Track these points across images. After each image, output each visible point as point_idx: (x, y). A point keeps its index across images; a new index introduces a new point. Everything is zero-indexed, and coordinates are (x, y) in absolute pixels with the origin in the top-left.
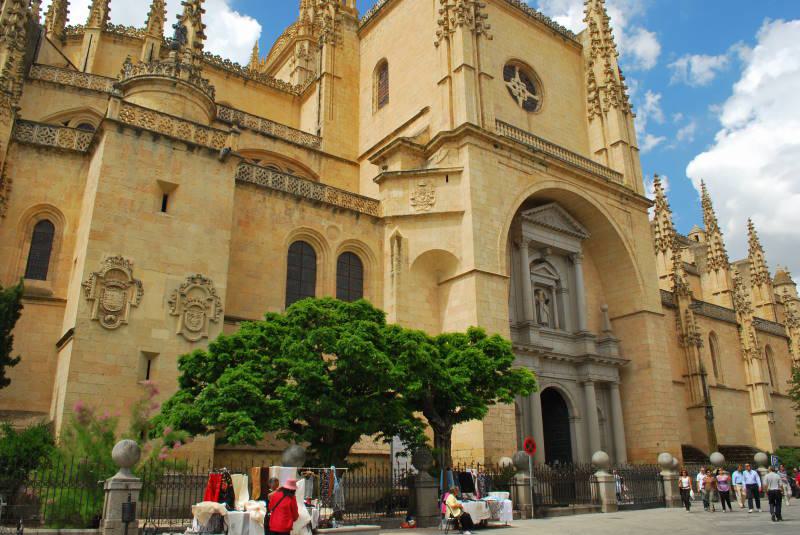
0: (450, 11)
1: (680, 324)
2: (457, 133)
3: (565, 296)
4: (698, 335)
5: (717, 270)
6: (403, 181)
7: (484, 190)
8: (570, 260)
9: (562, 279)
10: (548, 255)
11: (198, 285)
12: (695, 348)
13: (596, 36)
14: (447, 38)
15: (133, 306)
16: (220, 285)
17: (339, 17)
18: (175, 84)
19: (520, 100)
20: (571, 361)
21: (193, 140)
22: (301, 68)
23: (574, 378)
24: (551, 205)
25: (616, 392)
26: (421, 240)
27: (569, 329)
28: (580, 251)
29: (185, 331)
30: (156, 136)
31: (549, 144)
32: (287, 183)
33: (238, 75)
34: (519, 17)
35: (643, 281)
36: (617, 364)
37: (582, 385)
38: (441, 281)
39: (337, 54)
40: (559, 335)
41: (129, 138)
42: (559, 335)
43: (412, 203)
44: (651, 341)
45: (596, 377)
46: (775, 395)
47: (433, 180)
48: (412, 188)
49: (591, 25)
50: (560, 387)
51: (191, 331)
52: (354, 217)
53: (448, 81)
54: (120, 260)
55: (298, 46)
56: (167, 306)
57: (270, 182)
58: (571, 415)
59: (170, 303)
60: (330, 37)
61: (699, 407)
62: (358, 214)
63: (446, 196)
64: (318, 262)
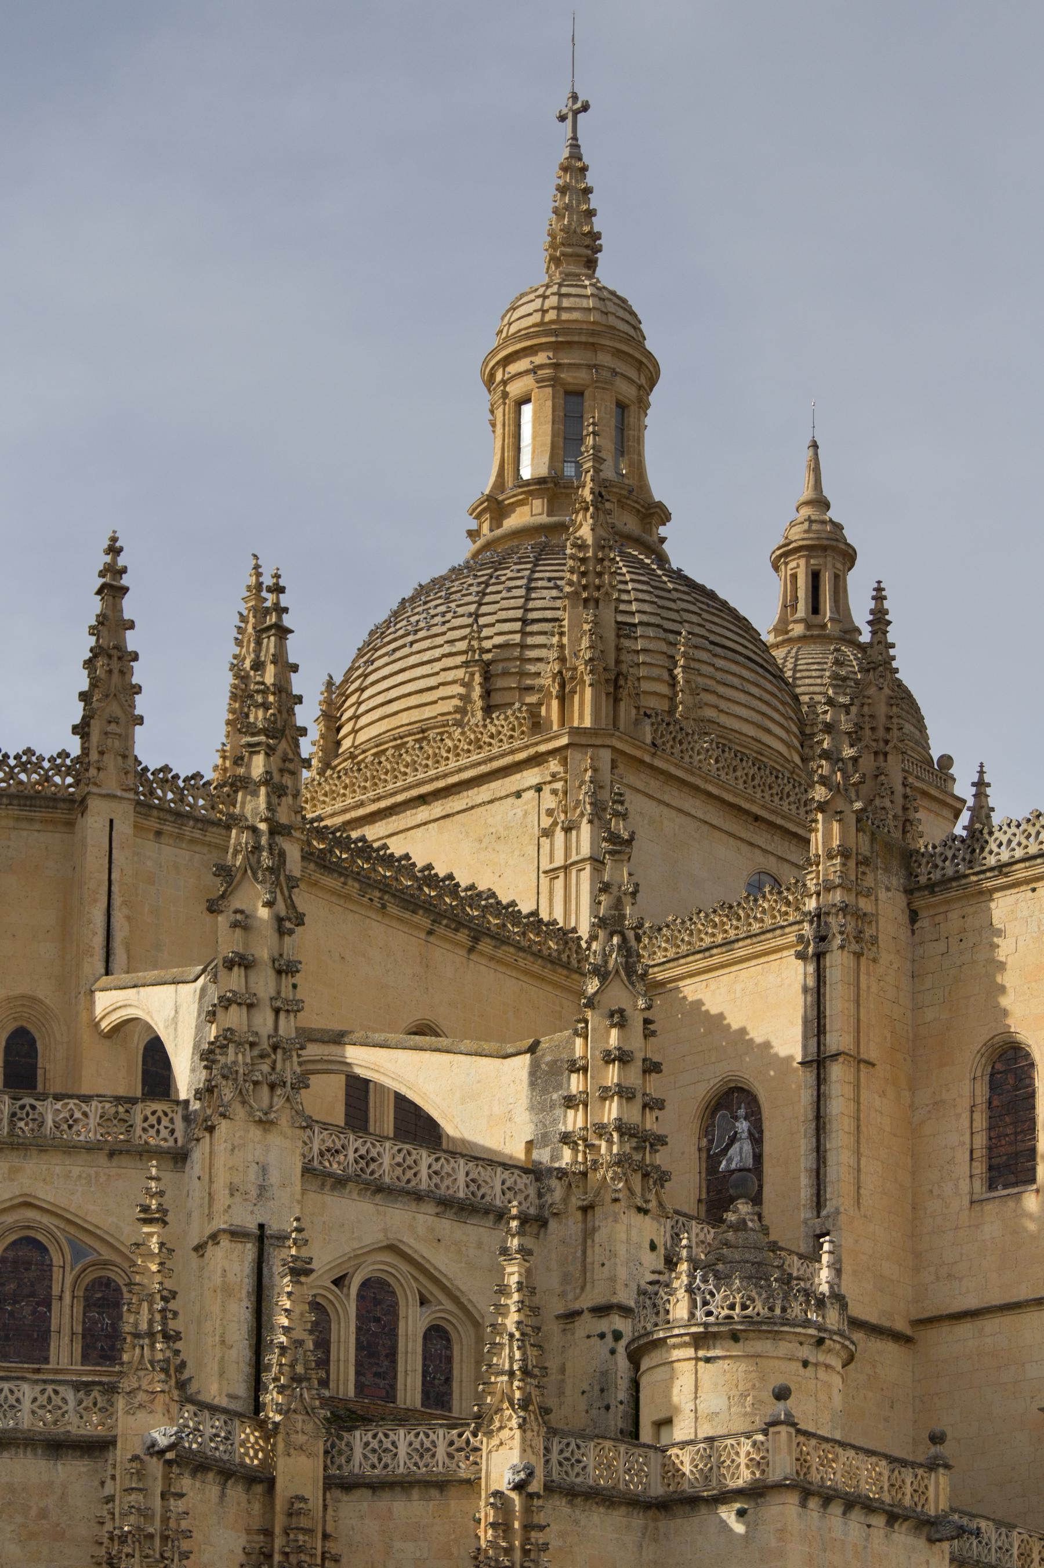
18: (820, 1342)
33: (458, 923)
39: (863, 978)
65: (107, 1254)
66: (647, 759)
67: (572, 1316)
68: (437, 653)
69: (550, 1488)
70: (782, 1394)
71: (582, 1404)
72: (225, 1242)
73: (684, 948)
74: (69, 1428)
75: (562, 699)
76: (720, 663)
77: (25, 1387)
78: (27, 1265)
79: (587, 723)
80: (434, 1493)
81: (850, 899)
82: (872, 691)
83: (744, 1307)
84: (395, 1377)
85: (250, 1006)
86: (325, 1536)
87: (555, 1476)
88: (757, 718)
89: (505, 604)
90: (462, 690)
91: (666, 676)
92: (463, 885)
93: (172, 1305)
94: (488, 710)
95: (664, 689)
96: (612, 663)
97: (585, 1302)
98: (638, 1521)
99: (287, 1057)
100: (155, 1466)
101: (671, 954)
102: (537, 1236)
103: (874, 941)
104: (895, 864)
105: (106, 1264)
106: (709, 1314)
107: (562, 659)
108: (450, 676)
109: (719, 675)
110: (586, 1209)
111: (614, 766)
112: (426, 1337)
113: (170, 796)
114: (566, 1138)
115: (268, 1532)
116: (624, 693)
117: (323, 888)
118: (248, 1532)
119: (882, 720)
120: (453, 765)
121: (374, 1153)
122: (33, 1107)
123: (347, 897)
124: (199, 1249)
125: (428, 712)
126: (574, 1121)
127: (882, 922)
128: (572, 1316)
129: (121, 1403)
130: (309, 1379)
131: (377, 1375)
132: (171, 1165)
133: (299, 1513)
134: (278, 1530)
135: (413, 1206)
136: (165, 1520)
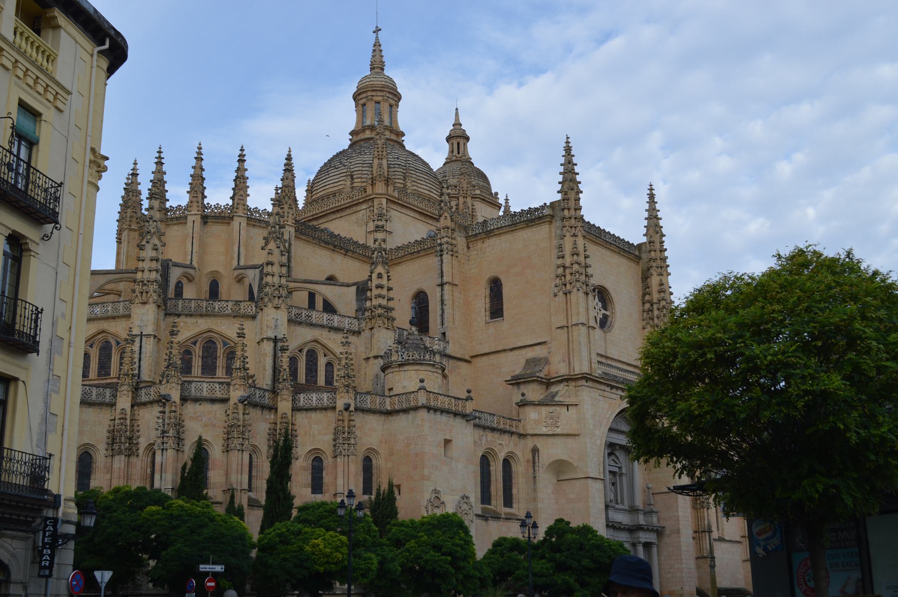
0: (568, 271)
2: (576, 377)
3: (624, 478)
6: (538, 408)
7: (592, 419)
8: (628, 450)
9: (623, 466)
10: (616, 450)
11: (465, 501)
12: (705, 509)
14: (566, 294)
16: (472, 500)
21: (454, 409)
23: (629, 540)
24: (620, 415)
26: (551, 451)
30: (443, 411)
31: (625, 371)
37: (634, 545)
38: (562, 478)
41: (432, 415)
43: (544, 424)
44: (680, 514)
45: (643, 540)
47: (558, 408)
48: (544, 410)
49: (650, 243)
52: (510, 435)
54: (436, 491)
55: (376, 202)
60: (450, 247)
61: (706, 557)
62: (512, 433)
63: (567, 420)
64: (492, 468)
66: (397, 201)
67: (367, 359)
68: (339, 172)
69: (356, 409)
70: (422, 381)
71: (371, 383)
72: (265, 341)
73: (406, 253)
74: (218, 396)
75: (372, 185)
76: (418, 174)
77: (205, 384)
78: (210, 348)
79: (380, 192)
80: (324, 411)
81: (450, 240)
82: (462, 180)
83: (413, 356)
84: (317, 377)
85: (273, 275)
86: (292, 424)
87: (358, 406)
88: (429, 189)
89: (357, 159)
90: (346, 183)
91: (402, 178)
92: (343, 237)
93: (246, 360)
94: (352, 188)
95: (401, 181)
96: (386, 176)
97: (372, 355)
98: (383, 418)
100: (240, 406)
101: (403, 254)
102: (358, 336)
103: (457, 252)
104: (462, 231)
106: (403, 358)
107: (372, 174)
108: (342, 179)
109: (418, 177)
110: (371, 329)
112: (326, 366)
113: (257, 215)
114: (365, 310)
115: (276, 424)
116: (389, 183)
118: (270, 423)
119: (465, 189)
120: (342, 203)
121: (310, 314)
122: (212, 304)
123: (309, 241)
124: (258, 343)
125: (336, 189)
126: (368, 304)
127: (459, 246)
128: (367, 359)
129: (231, 387)
130: (287, 380)
131: (311, 376)
132: (251, 320)
133: (285, 417)
134: (278, 423)
135: (322, 329)
136: (244, 421)
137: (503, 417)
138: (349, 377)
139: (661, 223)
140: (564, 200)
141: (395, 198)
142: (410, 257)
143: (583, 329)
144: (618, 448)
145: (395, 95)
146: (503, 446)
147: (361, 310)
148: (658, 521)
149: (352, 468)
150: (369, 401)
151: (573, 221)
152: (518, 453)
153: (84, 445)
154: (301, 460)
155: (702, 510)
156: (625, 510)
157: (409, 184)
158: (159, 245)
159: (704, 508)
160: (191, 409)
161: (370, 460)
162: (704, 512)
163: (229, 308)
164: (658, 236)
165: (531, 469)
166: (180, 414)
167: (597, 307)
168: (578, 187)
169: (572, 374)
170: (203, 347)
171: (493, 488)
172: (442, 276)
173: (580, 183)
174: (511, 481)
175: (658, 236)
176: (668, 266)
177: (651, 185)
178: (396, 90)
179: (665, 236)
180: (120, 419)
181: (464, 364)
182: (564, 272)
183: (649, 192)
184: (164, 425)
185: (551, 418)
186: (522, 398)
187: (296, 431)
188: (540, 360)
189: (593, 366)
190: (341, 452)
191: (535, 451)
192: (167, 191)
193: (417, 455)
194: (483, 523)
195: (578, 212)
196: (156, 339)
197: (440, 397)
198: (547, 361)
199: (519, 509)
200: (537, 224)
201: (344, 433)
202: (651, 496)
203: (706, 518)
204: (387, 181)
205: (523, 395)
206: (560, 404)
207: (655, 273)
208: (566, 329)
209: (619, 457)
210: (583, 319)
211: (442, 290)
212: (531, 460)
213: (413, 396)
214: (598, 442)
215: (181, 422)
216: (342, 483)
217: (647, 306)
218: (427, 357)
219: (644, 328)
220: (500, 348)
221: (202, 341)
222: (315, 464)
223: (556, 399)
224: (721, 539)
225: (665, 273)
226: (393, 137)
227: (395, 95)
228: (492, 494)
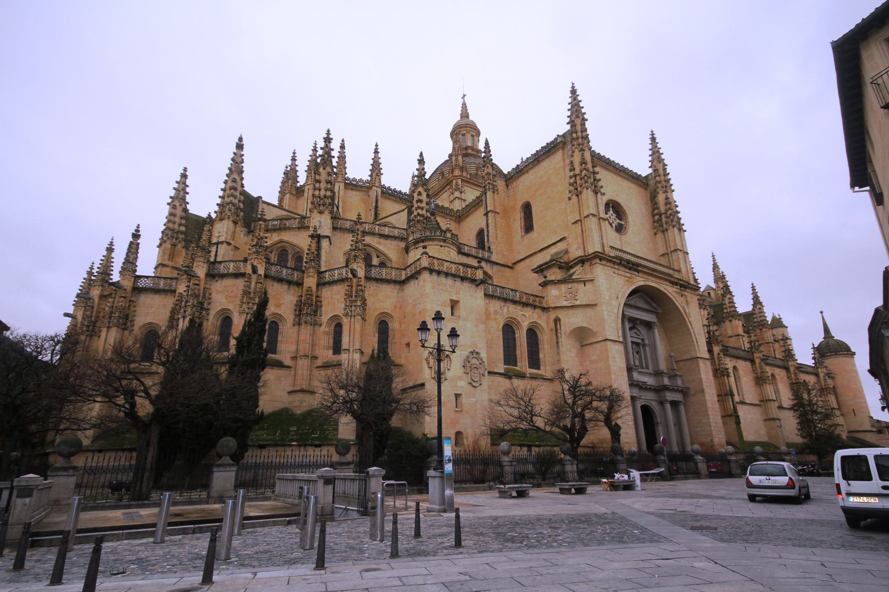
0: (578, 178)
1: (715, 362)
2: (590, 257)
3: (647, 348)
4: (727, 369)
5: (730, 321)
6: (559, 285)
9: (645, 338)
10: (637, 324)
11: (475, 356)
12: (726, 378)
13: (658, 178)
14: (577, 195)
15: (449, 370)
16: (484, 355)
17: (494, 173)
18: (445, 240)
19: (614, 225)
20: (655, 389)
21: (462, 275)
22: (459, 198)
23: (657, 399)
24: (639, 294)
25: (682, 407)
26: (572, 321)
27: (651, 370)
28: (655, 320)
29: (472, 381)
30: (447, 275)
32: (498, 292)
34: (611, 171)
35: (696, 338)
36: (682, 390)
37: (662, 403)
38: (583, 344)
39: (495, 197)
40: (646, 373)
41: (435, 277)
42: (646, 373)
43: (564, 298)
44: (703, 376)
46: (780, 407)
47: (576, 285)
48: (564, 288)
50: (649, 404)
51: (474, 381)
53: (579, 222)
55: (454, 182)
56: (462, 368)
57: (491, 291)
58: (655, 421)
59: (464, 366)
60: (491, 187)
61: (730, 416)
63: (584, 294)
64: (517, 335)
65: (299, 250)
69: (368, 278)
77: (232, 263)
80: (342, 283)
86: (317, 297)
96: (461, 165)
98: (398, 287)
99: (328, 198)
103: (497, 190)
105: (298, 252)
111: (462, 182)
115: (301, 296)
117: (391, 199)
118: (298, 297)
126: (413, 216)
136: (255, 289)
137: (526, 294)
138: (359, 250)
139: (663, 157)
140: (571, 127)
141: (468, 178)
142: (473, 209)
143: (594, 220)
144: (638, 322)
145: (475, 130)
146: (526, 318)
147: (409, 221)
148: (683, 383)
149: (358, 327)
150: (384, 273)
151: (580, 140)
152: (544, 324)
153: (149, 323)
154: (324, 326)
155: (722, 378)
156: (651, 374)
157: (479, 173)
158: (238, 178)
159: (724, 376)
160: (218, 286)
161: (387, 324)
162: (725, 380)
163: (296, 223)
164: (661, 165)
165: (554, 336)
166: (204, 288)
167: (612, 217)
168: (583, 116)
169: (587, 254)
170: (279, 254)
171: (518, 352)
172: (487, 207)
173: (585, 113)
174: (538, 347)
175: (661, 165)
176: (672, 185)
177: (652, 132)
178: (476, 127)
179: (667, 165)
180: (177, 300)
181: (507, 270)
182: (576, 179)
183: (651, 136)
184: (188, 296)
185: (570, 293)
186: (544, 280)
187: (321, 302)
188: (561, 252)
189: (606, 249)
190: (347, 313)
191: (557, 321)
192: (298, 177)
193: (420, 313)
194: (507, 381)
195: (584, 134)
196: (231, 247)
197: (446, 264)
198: (566, 252)
199: (545, 370)
200: (553, 153)
201: (352, 297)
202: (674, 363)
203: (727, 384)
204: (462, 169)
205: (545, 277)
206: (578, 281)
207: (661, 192)
208: (579, 222)
209: (642, 331)
210: (593, 211)
211: (487, 217)
212: (554, 328)
213: (419, 262)
214: (615, 311)
215: (207, 295)
216: (348, 340)
217: (657, 217)
218: (438, 233)
219: (655, 234)
220: (533, 252)
221: (277, 250)
222: (337, 329)
223: (574, 277)
224: (742, 403)
225: (669, 191)
226: (475, 153)
227: (475, 130)
228: (518, 357)
